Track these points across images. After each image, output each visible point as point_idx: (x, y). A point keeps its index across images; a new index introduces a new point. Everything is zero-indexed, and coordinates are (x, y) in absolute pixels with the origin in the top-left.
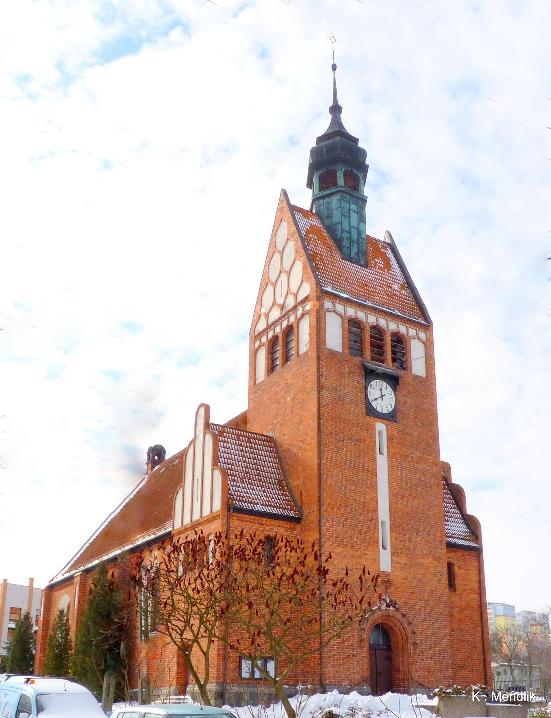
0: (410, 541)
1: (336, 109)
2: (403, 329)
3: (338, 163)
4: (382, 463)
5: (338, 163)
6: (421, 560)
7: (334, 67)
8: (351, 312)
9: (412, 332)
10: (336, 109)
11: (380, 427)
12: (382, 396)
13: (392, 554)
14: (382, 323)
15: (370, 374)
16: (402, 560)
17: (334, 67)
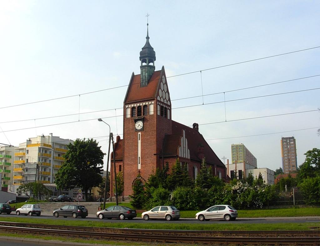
0: (146, 160)
1: (148, 38)
2: (147, 103)
3: (148, 54)
4: (140, 142)
5: (148, 54)
6: (149, 165)
7: (148, 24)
8: (132, 106)
9: (150, 103)
10: (148, 38)
11: (140, 133)
12: (139, 125)
13: (141, 165)
14: (141, 104)
15: (136, 121)
16: (143, 166)
17: (148, 24)
